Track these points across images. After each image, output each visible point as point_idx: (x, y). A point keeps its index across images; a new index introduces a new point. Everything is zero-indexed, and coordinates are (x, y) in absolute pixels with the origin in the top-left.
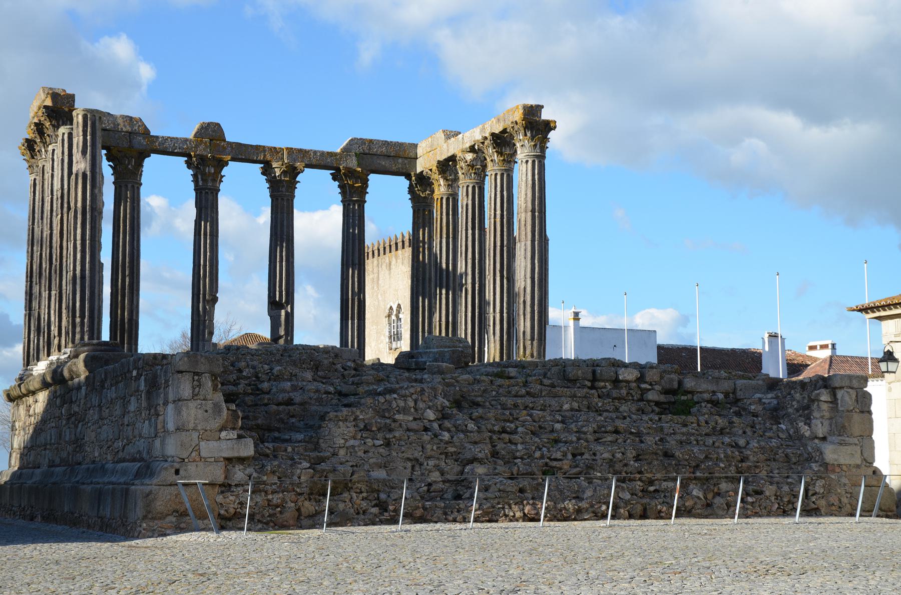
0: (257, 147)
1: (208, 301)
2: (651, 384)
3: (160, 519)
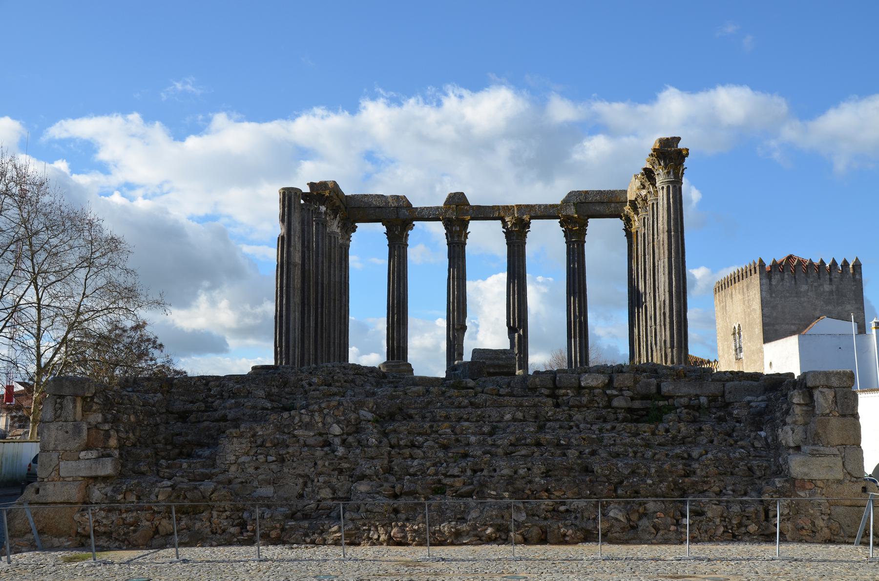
0: (493, 207)
1: (458, 330)
3: (19, 536)
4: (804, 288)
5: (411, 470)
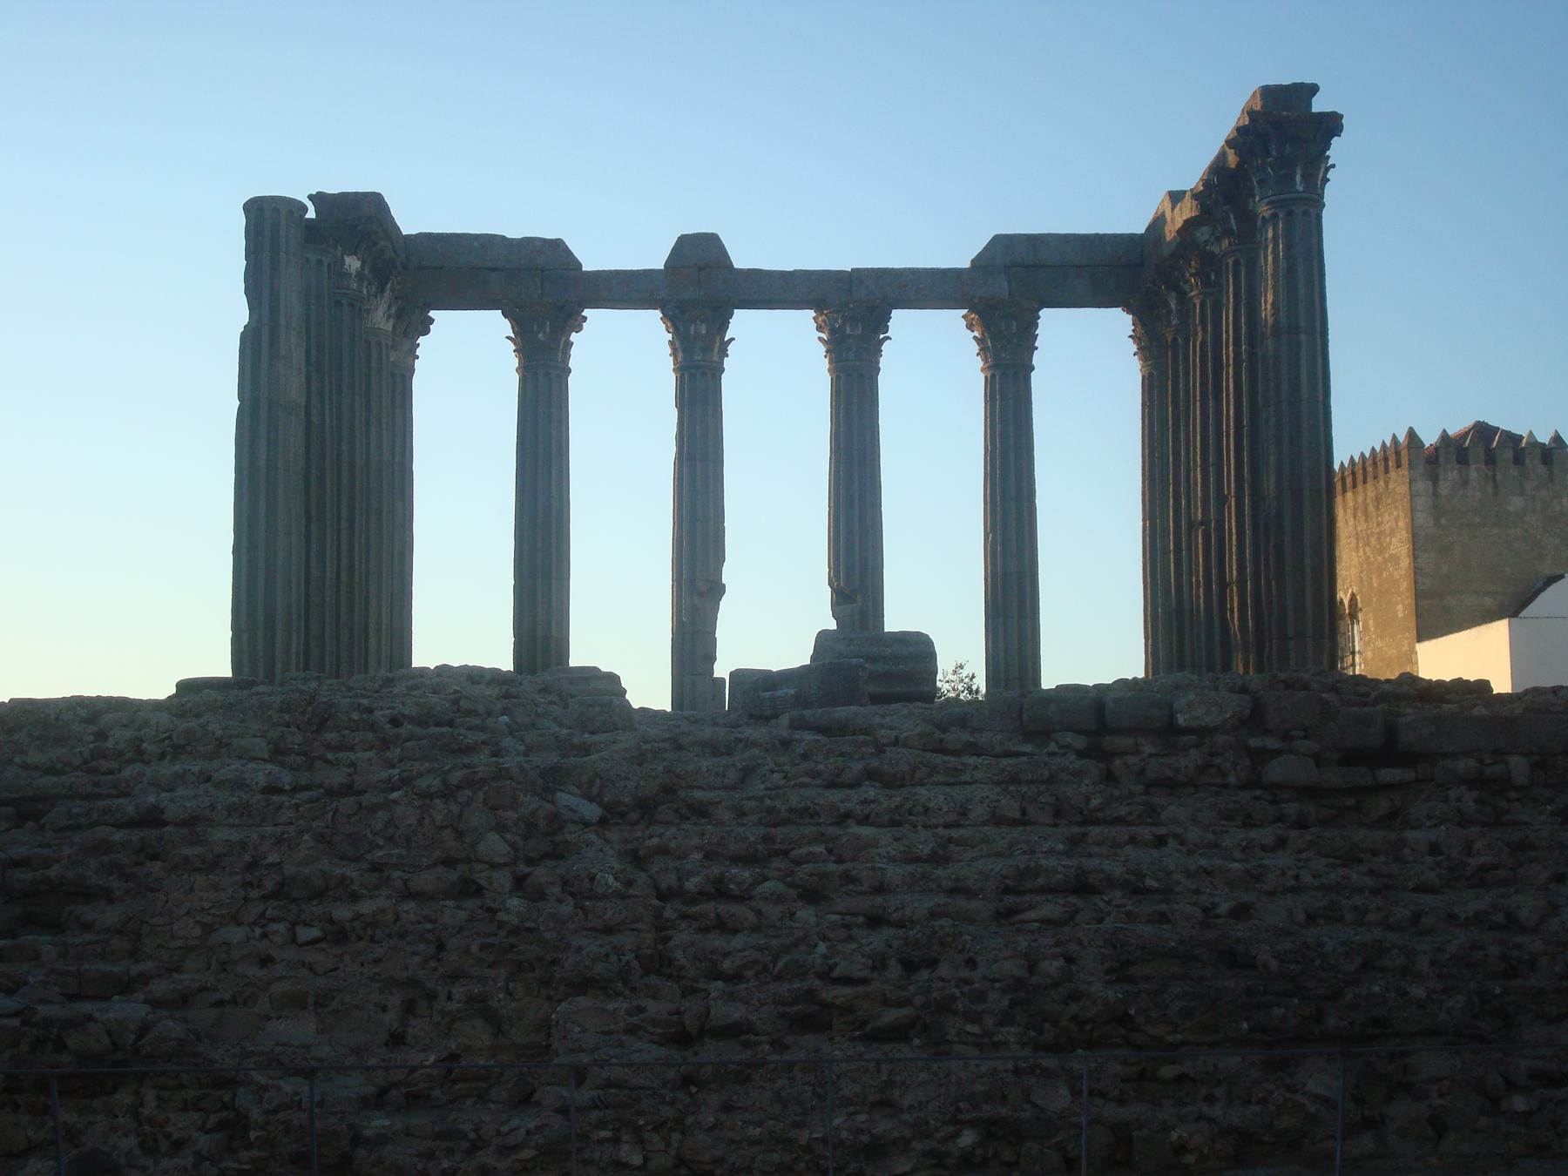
2: (1286, 737)
4: (1516, 503)
5: (727, 965)
